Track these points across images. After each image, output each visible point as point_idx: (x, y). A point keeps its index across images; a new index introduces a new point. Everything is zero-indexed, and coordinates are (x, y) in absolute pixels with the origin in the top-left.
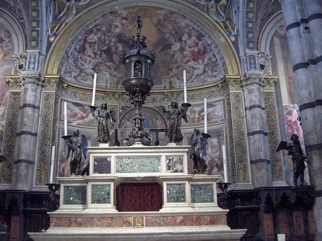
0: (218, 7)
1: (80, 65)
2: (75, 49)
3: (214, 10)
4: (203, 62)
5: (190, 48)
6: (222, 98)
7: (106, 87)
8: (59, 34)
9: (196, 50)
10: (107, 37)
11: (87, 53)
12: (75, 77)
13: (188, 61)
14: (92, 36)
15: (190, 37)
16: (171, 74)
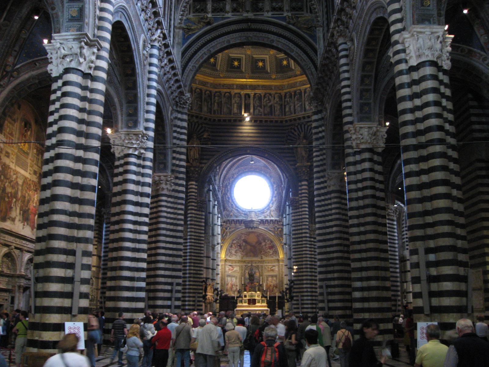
6: (277, 264)
15: (268, 241)
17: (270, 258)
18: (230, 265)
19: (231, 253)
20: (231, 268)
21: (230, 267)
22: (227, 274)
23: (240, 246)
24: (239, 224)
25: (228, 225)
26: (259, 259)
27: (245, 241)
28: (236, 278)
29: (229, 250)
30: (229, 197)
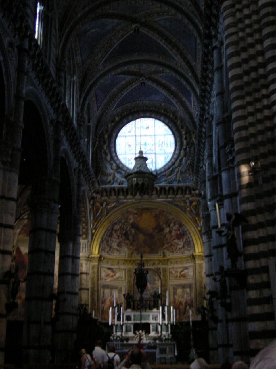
0: (192, 207)
1: (109, 244)
2: (107, 235)
3: (188, 209)
4: (183, 240)
5: (175, 231)
6: (192, 264)
7: (125, 256)
8: (98, 227)
9: (179, 233)
10: (125, 226)
11: (114, 236)
12: (108, 252)
13: (174, 239)
14: (116, 226)
15: (175, 225)
16: (164, 247)
17: (177, 255)
18: (109, 269)
19: (111, 247)
20: (111, 274)
21: (109, 272)
22: (102, 282)
23: (126, 235)
24: (123, 195)
25: (105, 198)
26: (161, 258)
27: (134, 226)
28: (120, 291)
29: (107, 241)
30: (107, 151)
